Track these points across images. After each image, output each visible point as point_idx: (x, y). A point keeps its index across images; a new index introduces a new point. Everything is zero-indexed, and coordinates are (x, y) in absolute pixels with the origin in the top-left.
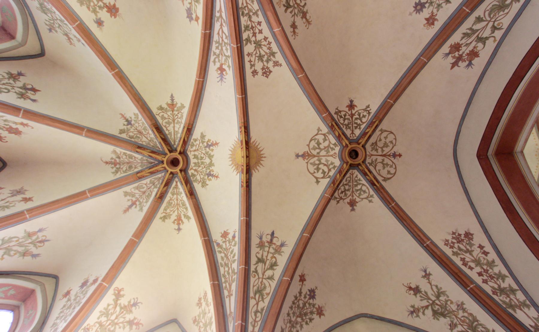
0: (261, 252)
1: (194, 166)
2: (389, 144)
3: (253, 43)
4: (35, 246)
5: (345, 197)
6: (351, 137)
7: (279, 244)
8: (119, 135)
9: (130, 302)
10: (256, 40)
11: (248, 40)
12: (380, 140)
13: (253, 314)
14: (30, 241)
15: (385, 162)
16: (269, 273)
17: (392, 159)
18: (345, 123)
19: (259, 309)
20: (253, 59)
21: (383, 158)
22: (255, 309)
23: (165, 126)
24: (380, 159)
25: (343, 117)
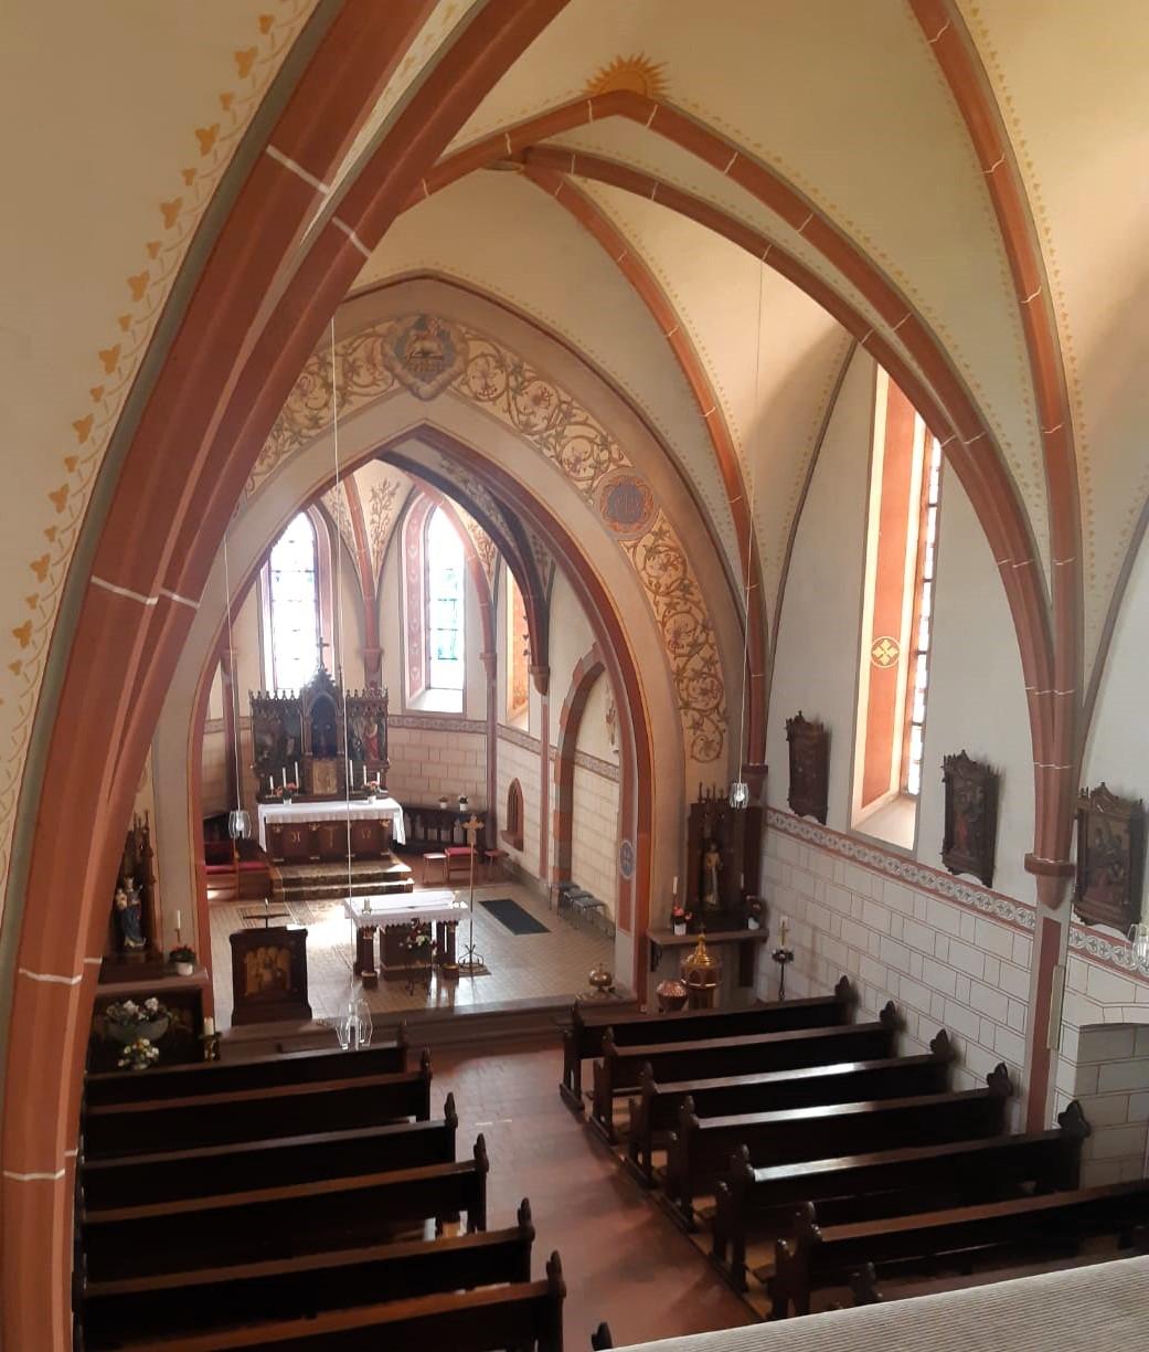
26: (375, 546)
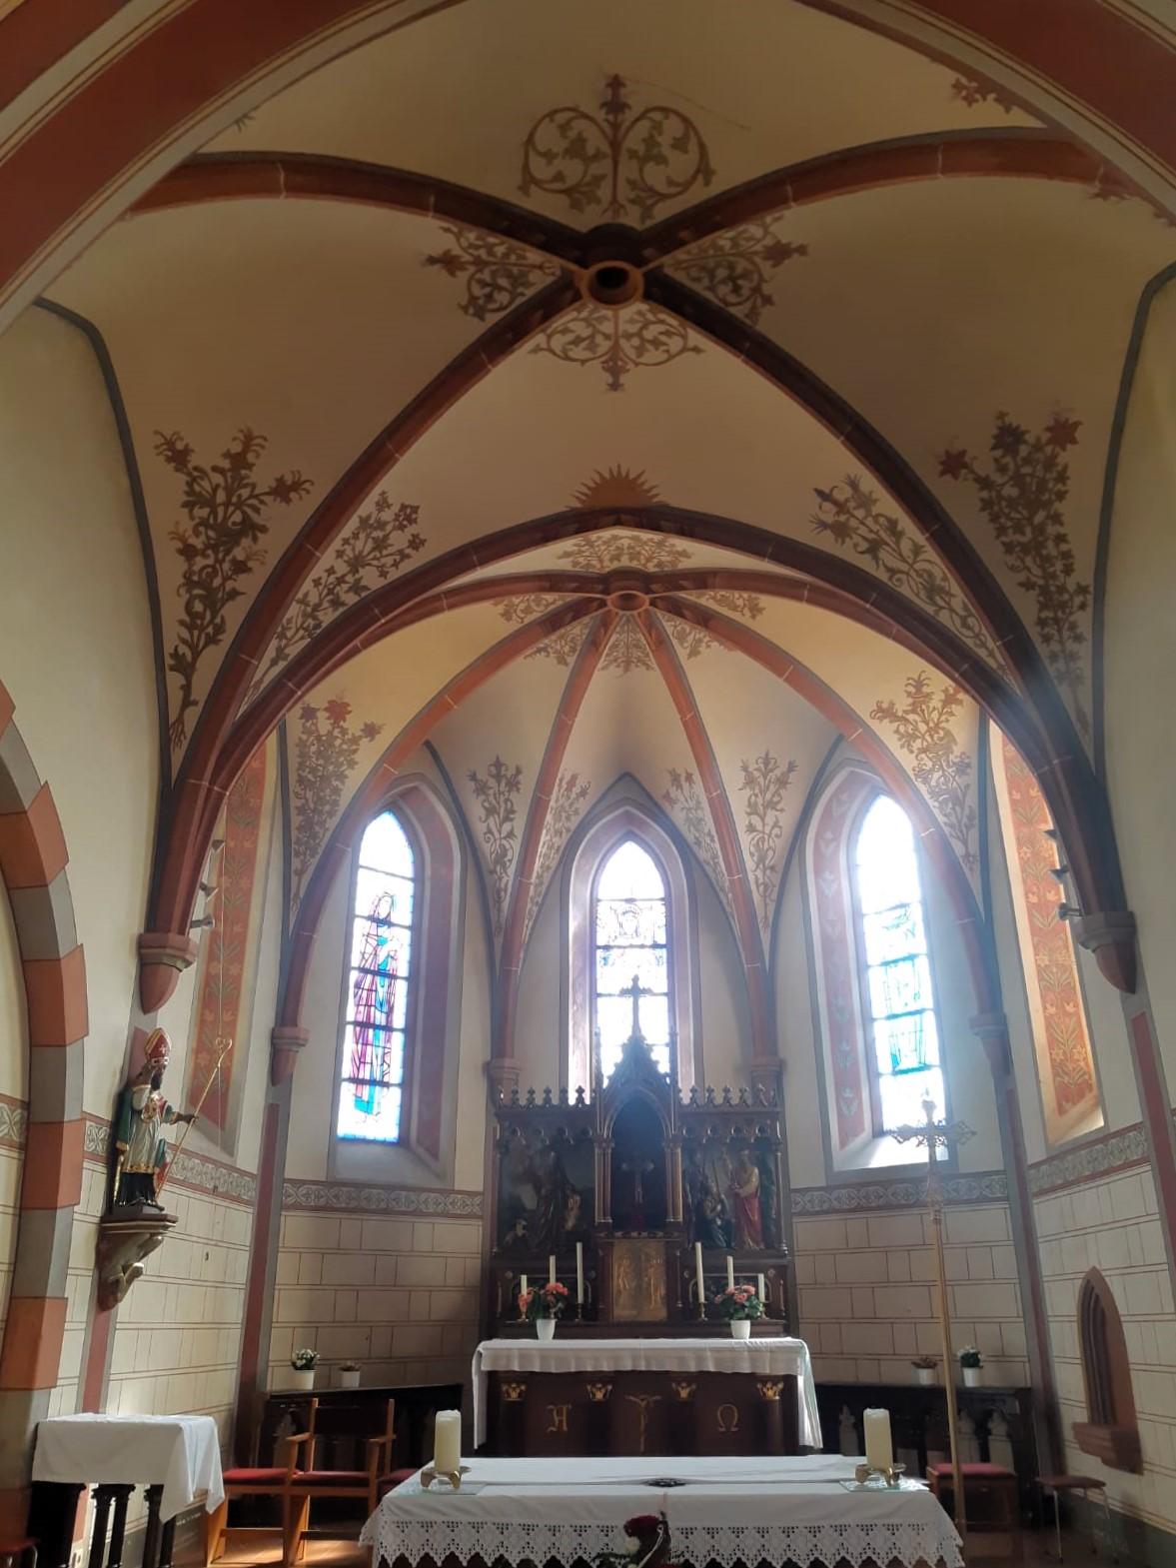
0: (856, 539)
1: (639, 560)
2: (572, 134)
3: (357, 576)
4: (772, 771)
5: (756, 276)
6: (553, 274)
7: (848, 492)
8: (571, 666)
9: (909, 694)
10: (349, 572)
11: (356, 588)
12: (559, 177)
13: (964, 631)
14: (761, 780)
15: (641, 149)
16: (906, 547)
17: (628, 116)
18: (508, 286)
19: (963, 613)
20: (389, 561)
21: (624, 158)
22: (958, 621)
23: (547, 606)
24: (628, 169)
25: (487, 290)
26: (759, 873)
